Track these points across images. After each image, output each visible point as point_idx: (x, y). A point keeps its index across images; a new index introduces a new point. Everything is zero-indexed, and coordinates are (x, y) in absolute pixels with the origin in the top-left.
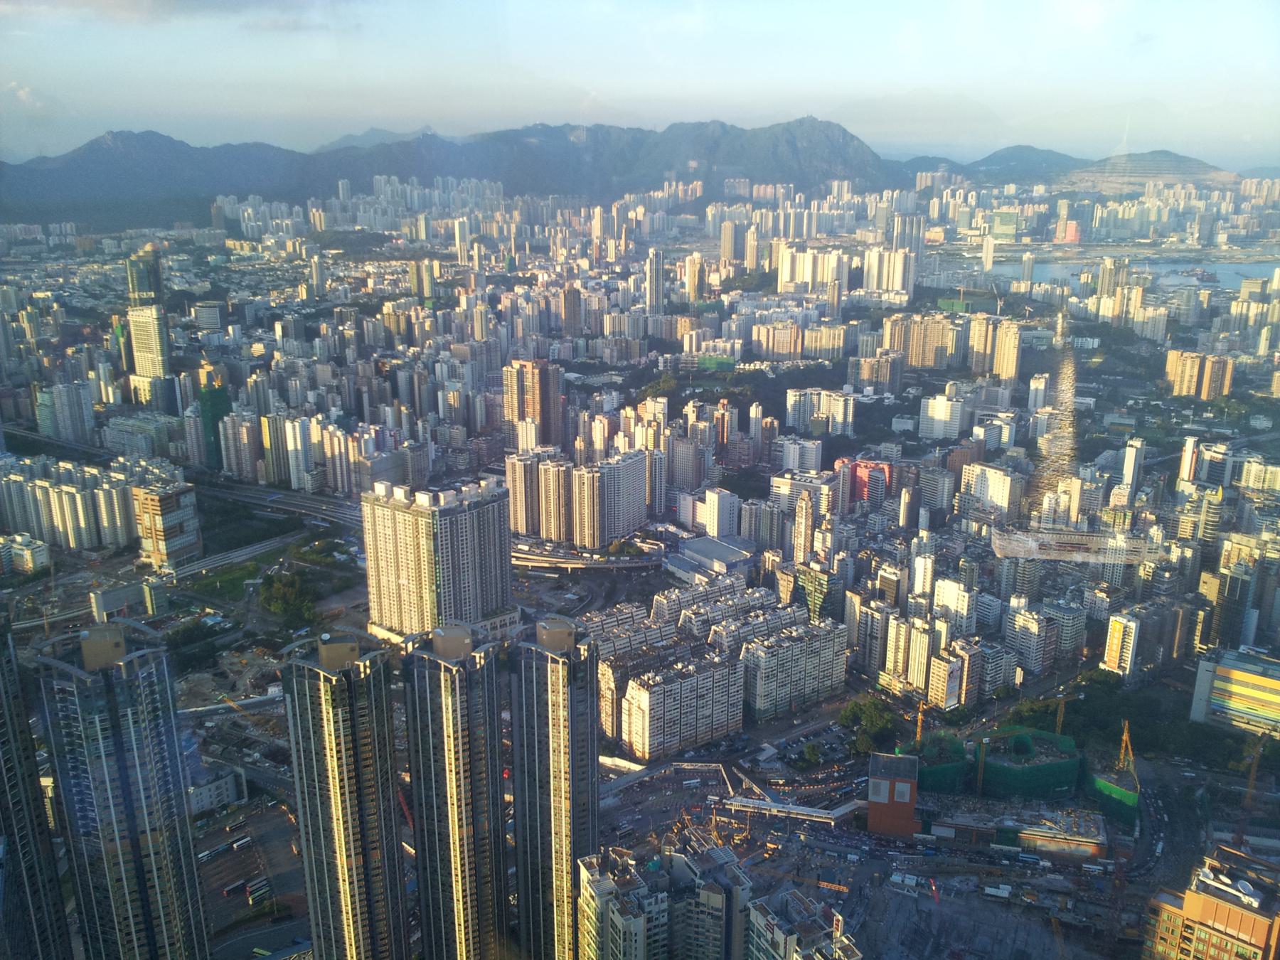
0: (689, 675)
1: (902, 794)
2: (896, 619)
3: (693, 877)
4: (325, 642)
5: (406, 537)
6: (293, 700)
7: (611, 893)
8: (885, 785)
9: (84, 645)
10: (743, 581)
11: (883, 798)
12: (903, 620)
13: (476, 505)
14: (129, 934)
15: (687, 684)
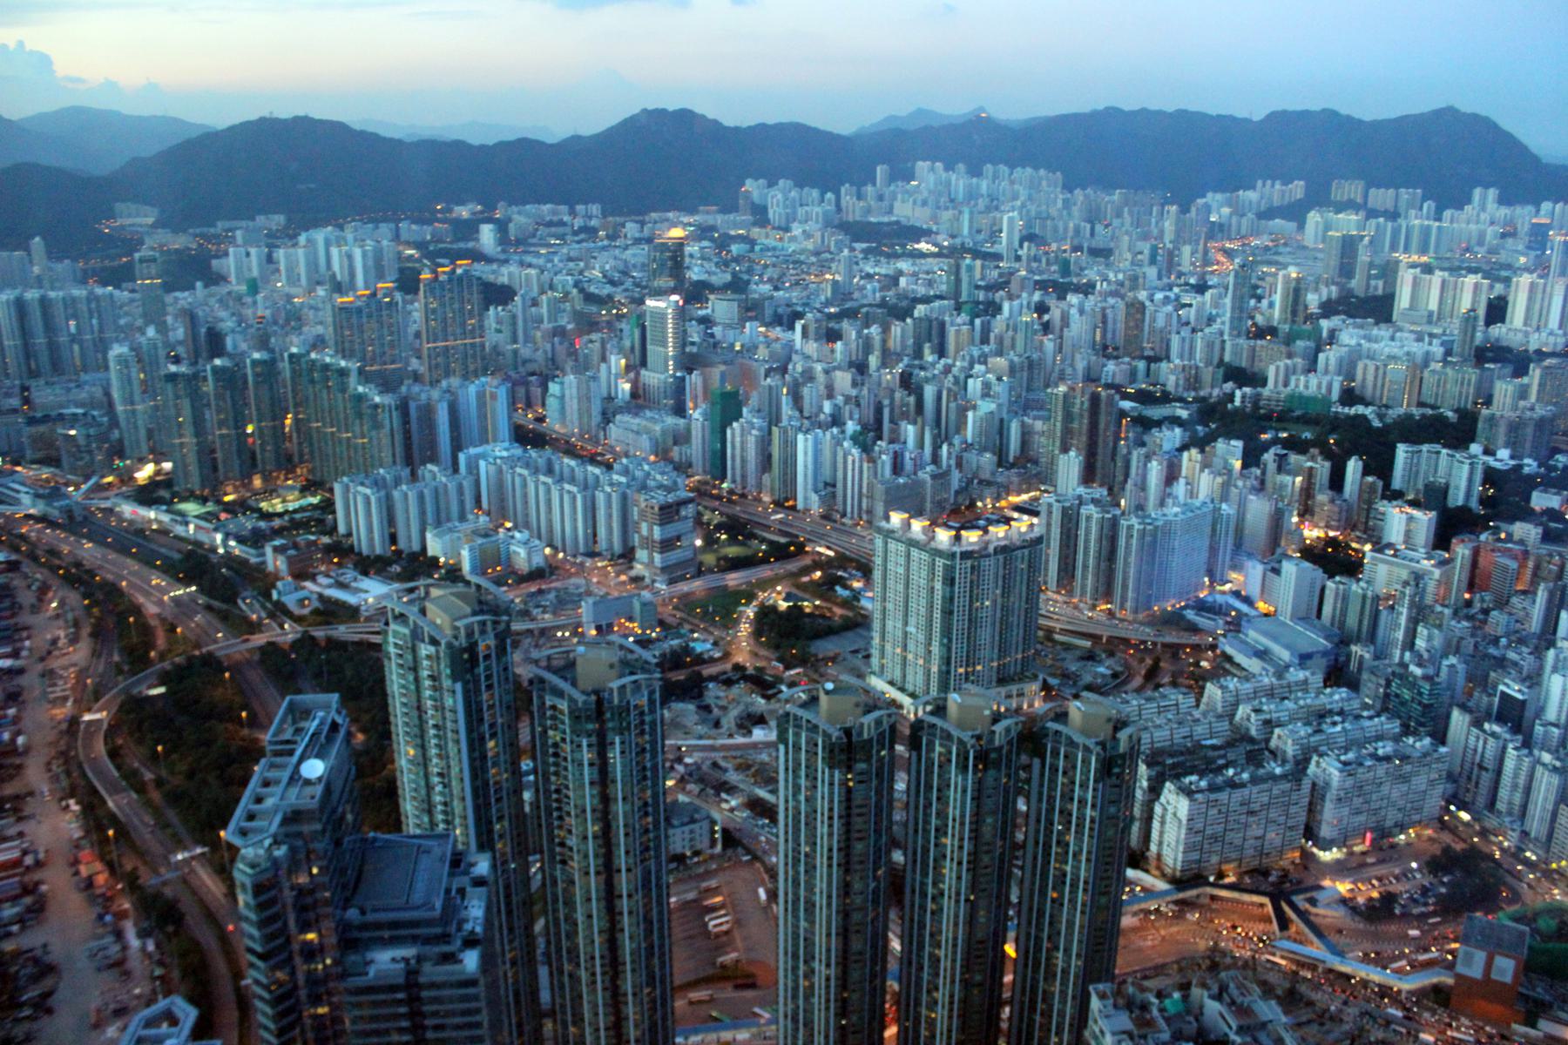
0: (1243, 785)
1: (1502, 972)
2: (1516, 749)
3: (1227, 1030)
4: (827, 692)
5: (919, 578)
6: (787, 753)
7: (1124, 1032)
8: (1480, 956)
9: (579, 661)
10: (1317, 679)
11: (1476, 972)
12: (1525, 751)
13: (1005, 550)
14: (594, 974)
15: (1238, 795)
